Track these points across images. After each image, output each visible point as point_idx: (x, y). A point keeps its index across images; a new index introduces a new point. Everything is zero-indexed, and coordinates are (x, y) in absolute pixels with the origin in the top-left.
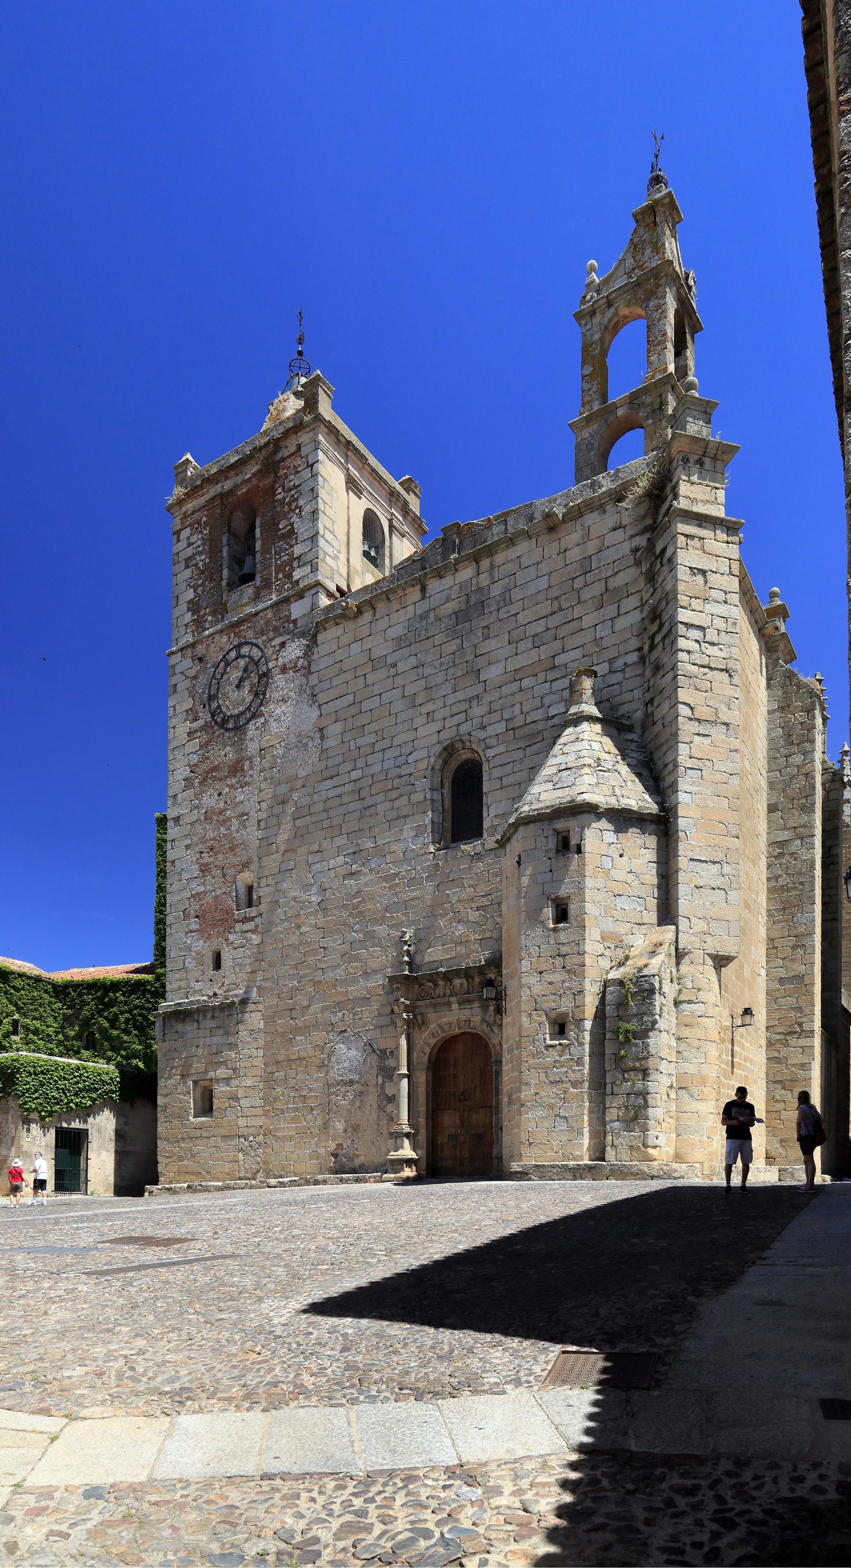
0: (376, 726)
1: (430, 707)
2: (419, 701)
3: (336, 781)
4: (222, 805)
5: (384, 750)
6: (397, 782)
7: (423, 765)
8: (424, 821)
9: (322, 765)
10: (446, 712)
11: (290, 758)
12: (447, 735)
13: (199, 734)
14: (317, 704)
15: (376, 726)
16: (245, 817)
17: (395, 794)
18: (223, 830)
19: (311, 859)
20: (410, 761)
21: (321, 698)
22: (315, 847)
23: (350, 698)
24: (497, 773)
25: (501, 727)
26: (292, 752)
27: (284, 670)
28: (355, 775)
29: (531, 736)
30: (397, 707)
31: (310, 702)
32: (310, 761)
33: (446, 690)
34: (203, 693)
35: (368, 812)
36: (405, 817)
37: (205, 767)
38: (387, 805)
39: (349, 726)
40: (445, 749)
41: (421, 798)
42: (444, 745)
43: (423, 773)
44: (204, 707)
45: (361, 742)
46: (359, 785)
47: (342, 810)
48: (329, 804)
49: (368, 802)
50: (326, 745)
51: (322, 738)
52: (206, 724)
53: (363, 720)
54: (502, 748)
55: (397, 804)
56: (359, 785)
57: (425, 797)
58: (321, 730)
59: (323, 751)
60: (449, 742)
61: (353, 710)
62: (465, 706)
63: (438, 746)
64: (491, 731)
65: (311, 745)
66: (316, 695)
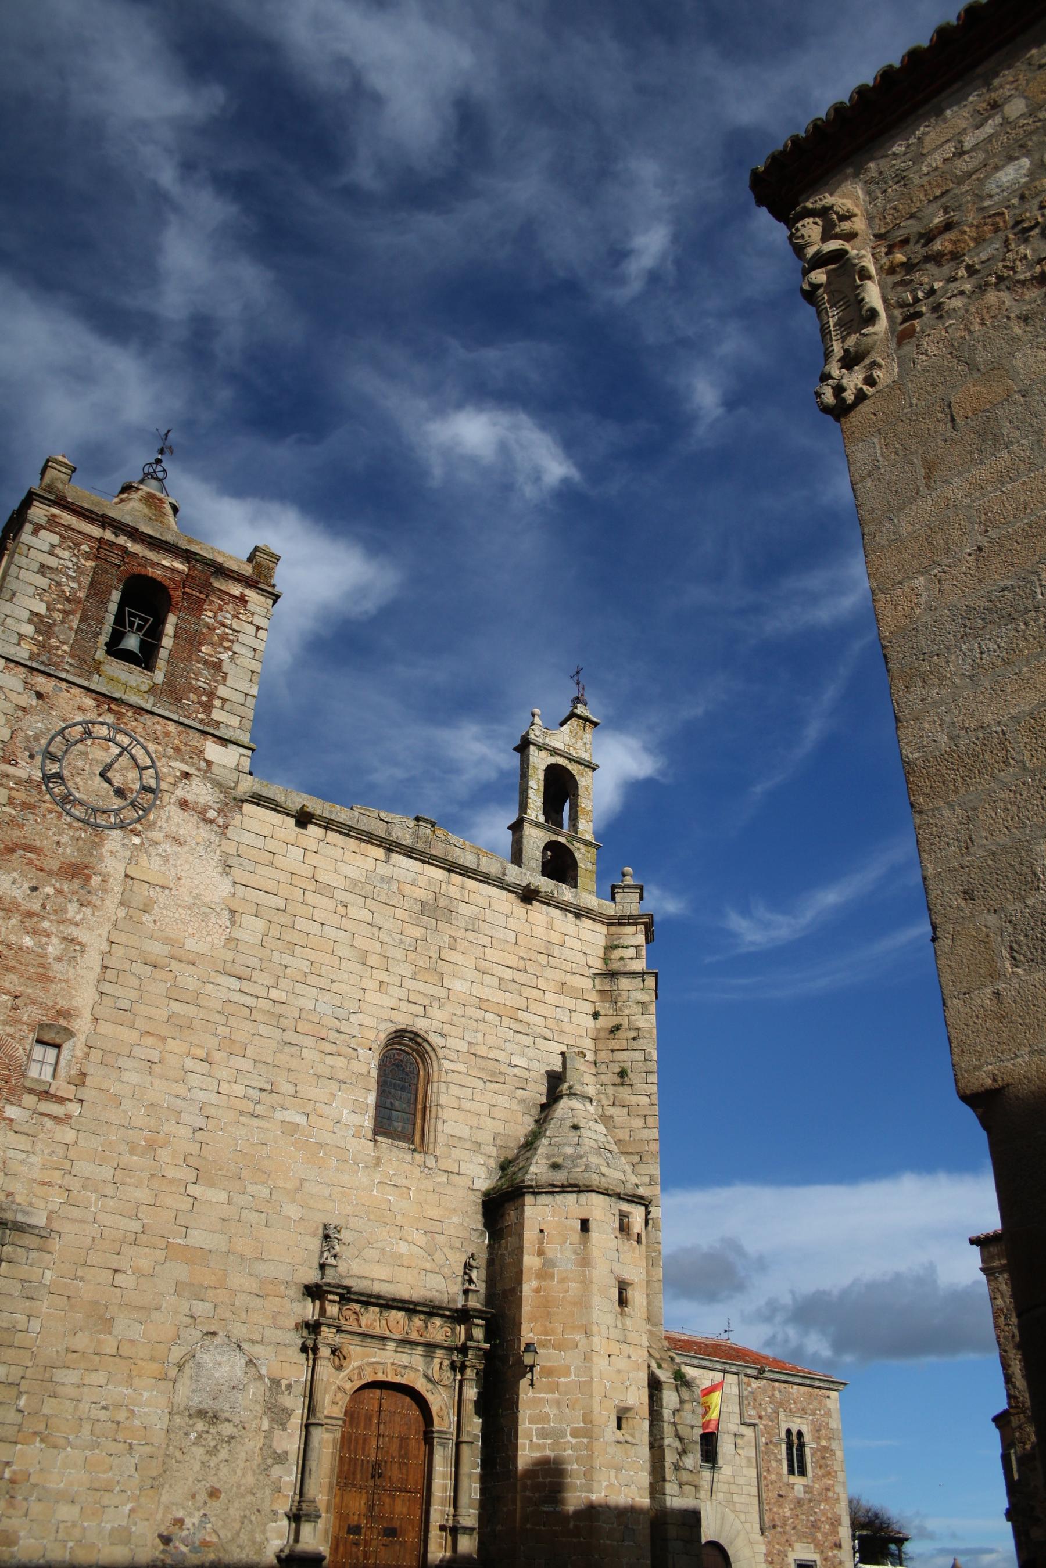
0: (313, 955)
1: (383, 976)
2: (373, 960)
3: (246, 986)
4: (36, 907)
5: (321, 989)
6: (333, 1035)
7: (371, 1035)
8: (366, 1098)
9: (230, 955)
10: (404, 995)
11: (177, 915)
12: (403, 1021)
13: (12, 784)
14: (231, 878)
15: (313, 955)
16: (78, 947)
17: (329, 1048)
18: (28, 941)
19: (189, 1063)
20: (351, 1020)
21: (237, 874)
22: (201, 1053)
23: (281, 904)
24: (454, 1090)
25: (463, 1046)
26: (180, 910)
27: (184, 804)
28: (274, 994)
29: (493, 1073)
30: (343, 951)
31: (220, 869)
32: (209, 939)
33: (407, 970)
34: (36, 738)
35: (288, 1049)
36: (340, 1081)
37: (15, 834)
38: (315, 1055)
39: (275, 931)
40: (396, 1031)
41: (364, 1071)
42: (398, 1028)
43: (370, 1045)
44: (32, 756)
45: (288, 960)
46: (278, 1009)
47: (249, 1026)
48: (230, 1009)
49: (290, 1036)
50: (237, 934)
51: (233, 922)
52: (29, 780)
53: (295, 937)
54: (461, 1068)
55: (330, 1060)
56: (278, 1009)
57: (369, 1072)
58: (233, 912)
59: (231, 939)
60: (404, 1027)
61: (284, 919)
62: (427, 1002)
63: (390, 1024)
64: (451, 1042)
65: (213, 920)
66: (231, 867)
